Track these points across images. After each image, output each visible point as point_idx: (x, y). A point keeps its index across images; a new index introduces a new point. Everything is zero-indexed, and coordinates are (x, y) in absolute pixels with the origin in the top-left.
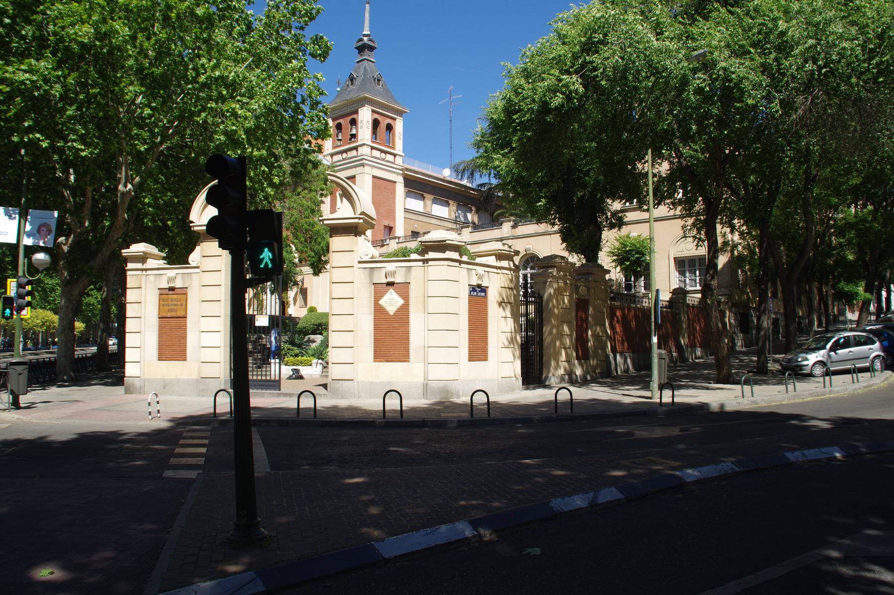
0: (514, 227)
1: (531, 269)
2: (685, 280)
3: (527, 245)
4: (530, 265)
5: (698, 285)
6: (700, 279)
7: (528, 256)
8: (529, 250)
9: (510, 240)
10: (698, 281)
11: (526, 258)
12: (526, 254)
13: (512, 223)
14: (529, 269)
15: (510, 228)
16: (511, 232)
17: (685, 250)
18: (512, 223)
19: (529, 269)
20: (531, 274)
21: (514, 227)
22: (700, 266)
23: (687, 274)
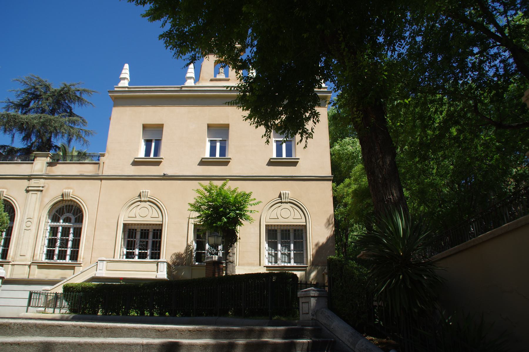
0: (50, 164)
1: (64, 221)
2: (276, 255)
3: (66, 188)
4: (64, 216)
5: (292, 261)
6: (294, 254)
7: (64, 204)
8: (68, 195)
9: (42, 180)
10: (292, 255)
11: (60, 205)
12: (63, 200)
13: (49, 160)
14: (61, 221)
15: (45, 165)
16: (46, 169)
17: (279, 216)
18: (49, 160)
19: (61, 221)
20: (63, 228)
21: (50, 164)
22: (295, 238)
23: (279, 246)
